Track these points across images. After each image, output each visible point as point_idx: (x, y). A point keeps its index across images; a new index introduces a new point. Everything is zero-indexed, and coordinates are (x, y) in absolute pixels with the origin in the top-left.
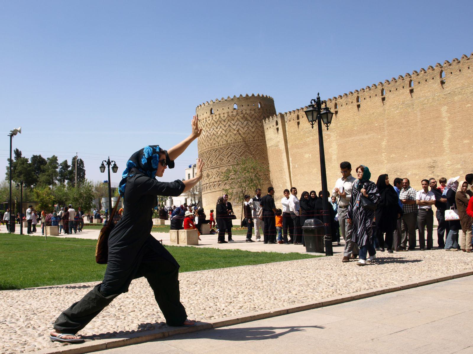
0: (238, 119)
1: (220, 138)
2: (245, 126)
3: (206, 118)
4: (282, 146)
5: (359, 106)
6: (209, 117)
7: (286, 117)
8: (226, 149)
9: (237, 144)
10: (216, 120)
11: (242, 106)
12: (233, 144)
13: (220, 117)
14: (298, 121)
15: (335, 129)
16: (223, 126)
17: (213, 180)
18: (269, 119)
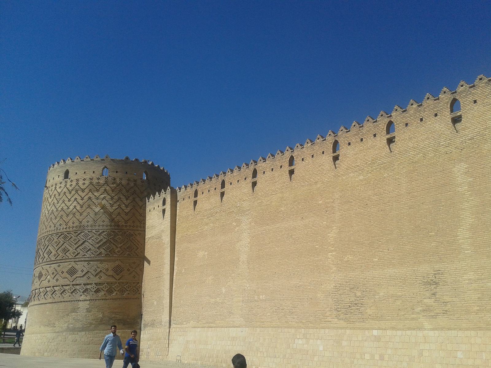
0: (105, 190)
1: (71, 216)
2: (115, 202)
3: (56, 185)
4: (167, 239)
5: (291, 172)
6: (61, 183)
7: (179, 194)
8: (77, 234)
9: (97, 228)
10: (70, 188)
11: (117, 172)
12: (89, 228)
13: (77, 184)
14: (195, 199)
15: (249, 210)
16: (79, 198)
17: (45, 283)
18: (154, 197)
